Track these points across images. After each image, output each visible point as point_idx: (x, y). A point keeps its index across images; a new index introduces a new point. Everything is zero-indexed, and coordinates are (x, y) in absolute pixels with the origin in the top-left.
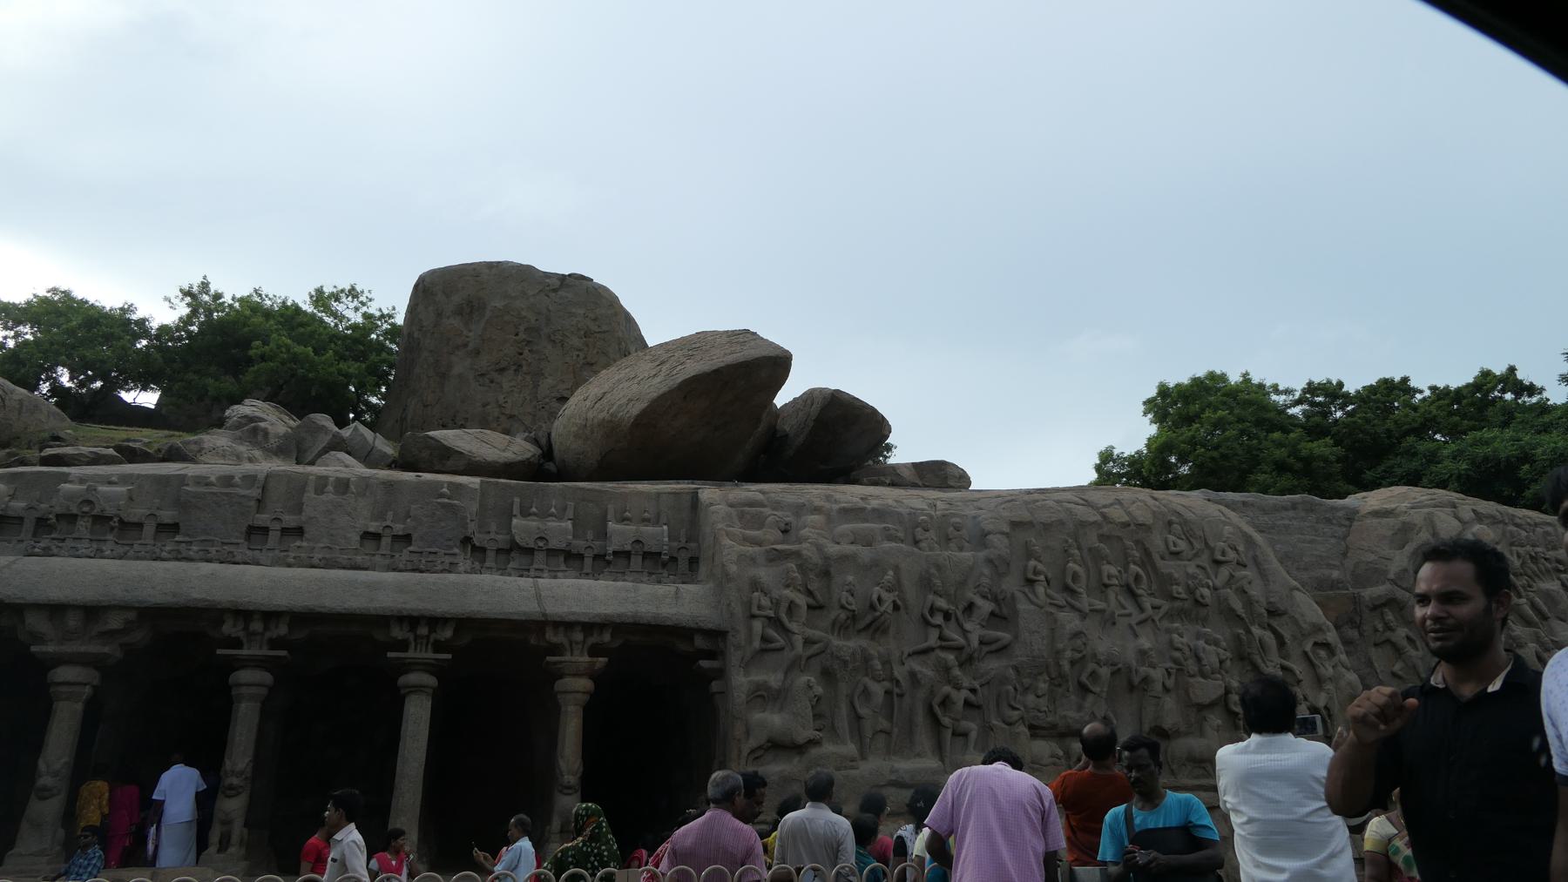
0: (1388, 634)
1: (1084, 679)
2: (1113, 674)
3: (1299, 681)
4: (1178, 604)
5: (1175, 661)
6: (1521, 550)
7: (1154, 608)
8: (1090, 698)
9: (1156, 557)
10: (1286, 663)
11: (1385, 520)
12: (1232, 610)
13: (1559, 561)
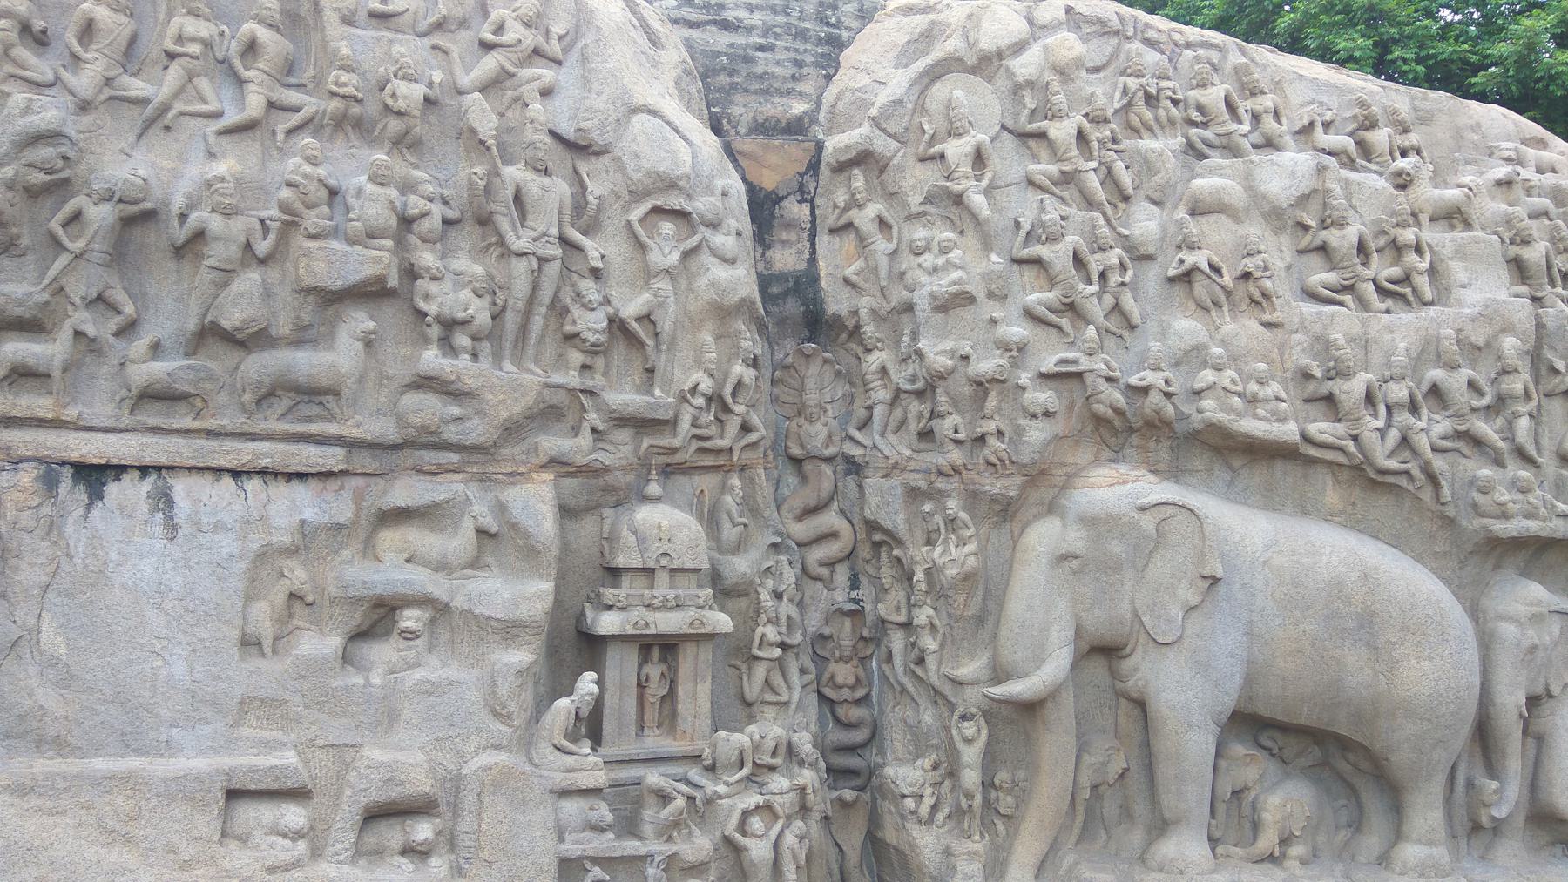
0: (853, 213)
1: (55, 225)
2: (128, 222)
3: (596, 274)
4: (335, 105)
5: (284, 207)
6: (1132, 83)
7: (271, 105)
8: (64, 259)
9: (331, 19)
10: (575, 235)
11: (906, 20)
12: (473, 131)
13: (1200, 108)
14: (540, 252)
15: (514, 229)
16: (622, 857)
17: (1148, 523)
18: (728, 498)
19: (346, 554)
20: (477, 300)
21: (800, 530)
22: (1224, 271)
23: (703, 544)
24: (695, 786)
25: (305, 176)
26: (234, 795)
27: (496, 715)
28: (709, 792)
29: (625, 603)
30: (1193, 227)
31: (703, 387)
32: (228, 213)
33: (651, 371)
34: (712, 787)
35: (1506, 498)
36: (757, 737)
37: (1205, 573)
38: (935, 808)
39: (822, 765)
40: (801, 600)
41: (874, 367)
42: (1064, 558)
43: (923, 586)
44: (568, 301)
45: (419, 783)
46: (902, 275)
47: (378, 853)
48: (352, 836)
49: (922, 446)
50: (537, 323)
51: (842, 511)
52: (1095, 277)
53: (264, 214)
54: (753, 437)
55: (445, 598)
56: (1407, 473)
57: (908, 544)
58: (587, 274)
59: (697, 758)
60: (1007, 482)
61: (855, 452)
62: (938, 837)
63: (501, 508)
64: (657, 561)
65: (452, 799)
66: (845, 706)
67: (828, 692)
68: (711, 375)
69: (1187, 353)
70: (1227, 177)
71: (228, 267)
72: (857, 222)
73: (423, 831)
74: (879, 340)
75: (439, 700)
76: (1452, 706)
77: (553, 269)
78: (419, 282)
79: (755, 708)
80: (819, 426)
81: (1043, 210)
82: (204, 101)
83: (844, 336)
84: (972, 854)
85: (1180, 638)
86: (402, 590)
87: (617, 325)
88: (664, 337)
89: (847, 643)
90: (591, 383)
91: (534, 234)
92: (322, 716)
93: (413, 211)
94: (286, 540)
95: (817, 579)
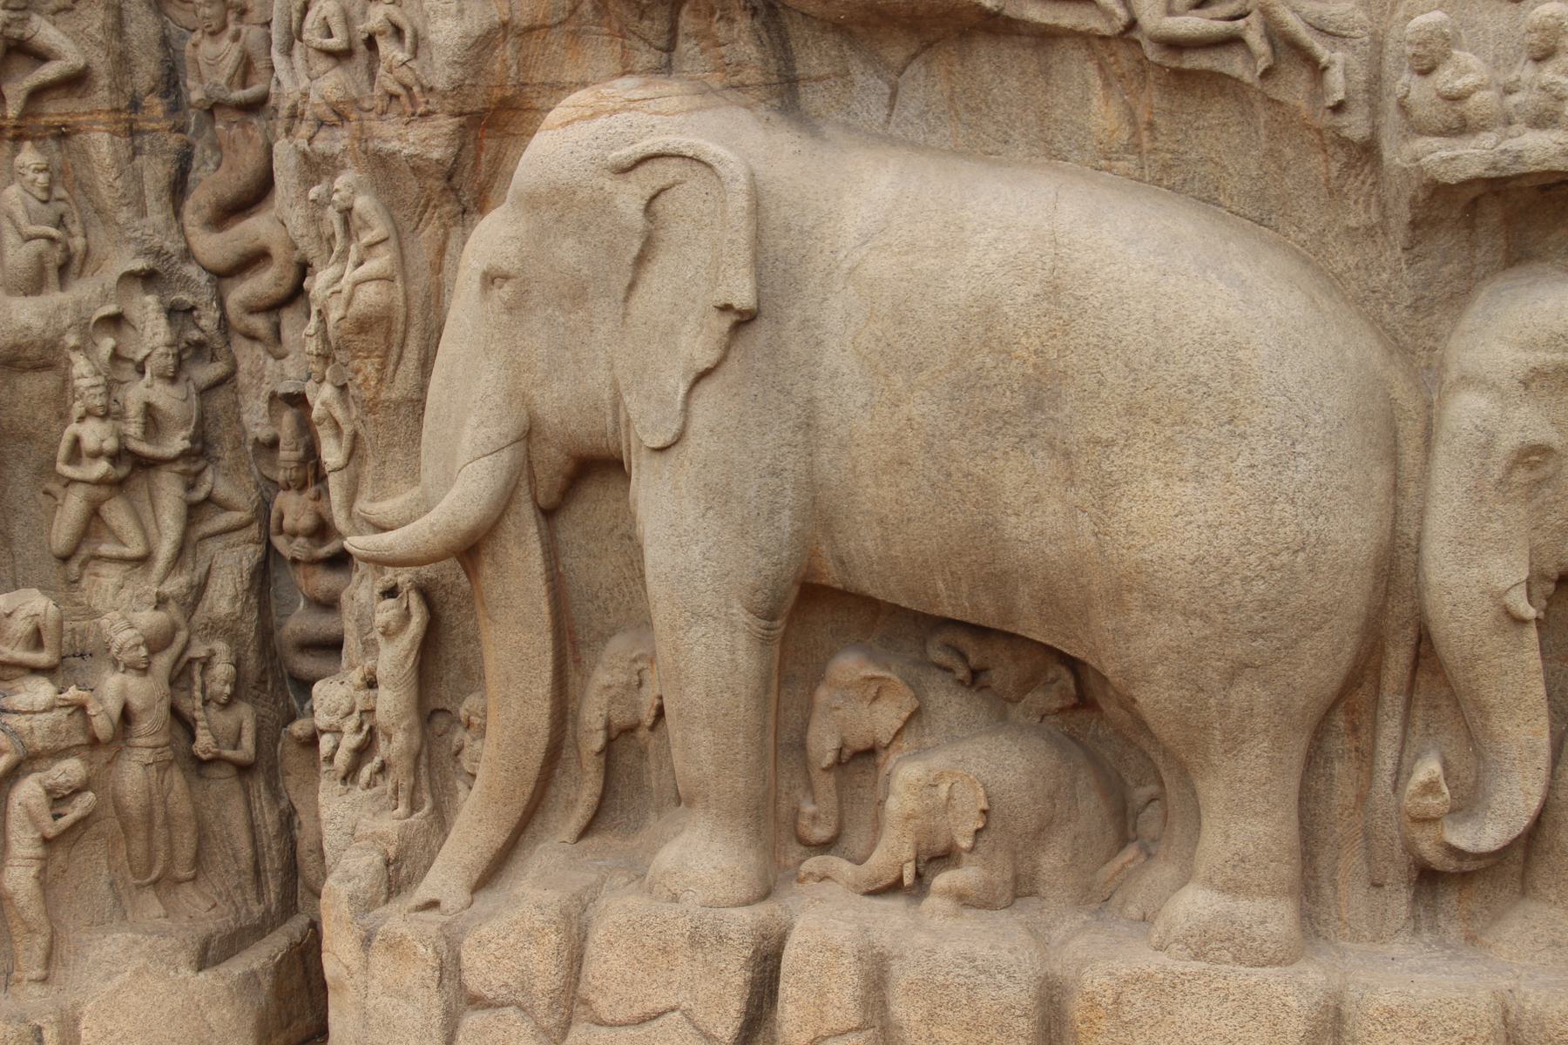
17: (629, 197)
21: (215, 247)
35: (1470, 80)
37: (721, 297)
38: (362, 752)
39: (222, 669)
40: (227, 380)
42: (491, 279)
43: (313, 345)
54: (49, 72)
56: (1232, 41)
57: (316, 263)
62: (353, 806)
66: (300, 570)
67: (280, 542)
76: (1259, 587)
79: (74, 567)
80: (225, 42)
85: (679, 438)
89: (287, 454)
95: (252, 337)
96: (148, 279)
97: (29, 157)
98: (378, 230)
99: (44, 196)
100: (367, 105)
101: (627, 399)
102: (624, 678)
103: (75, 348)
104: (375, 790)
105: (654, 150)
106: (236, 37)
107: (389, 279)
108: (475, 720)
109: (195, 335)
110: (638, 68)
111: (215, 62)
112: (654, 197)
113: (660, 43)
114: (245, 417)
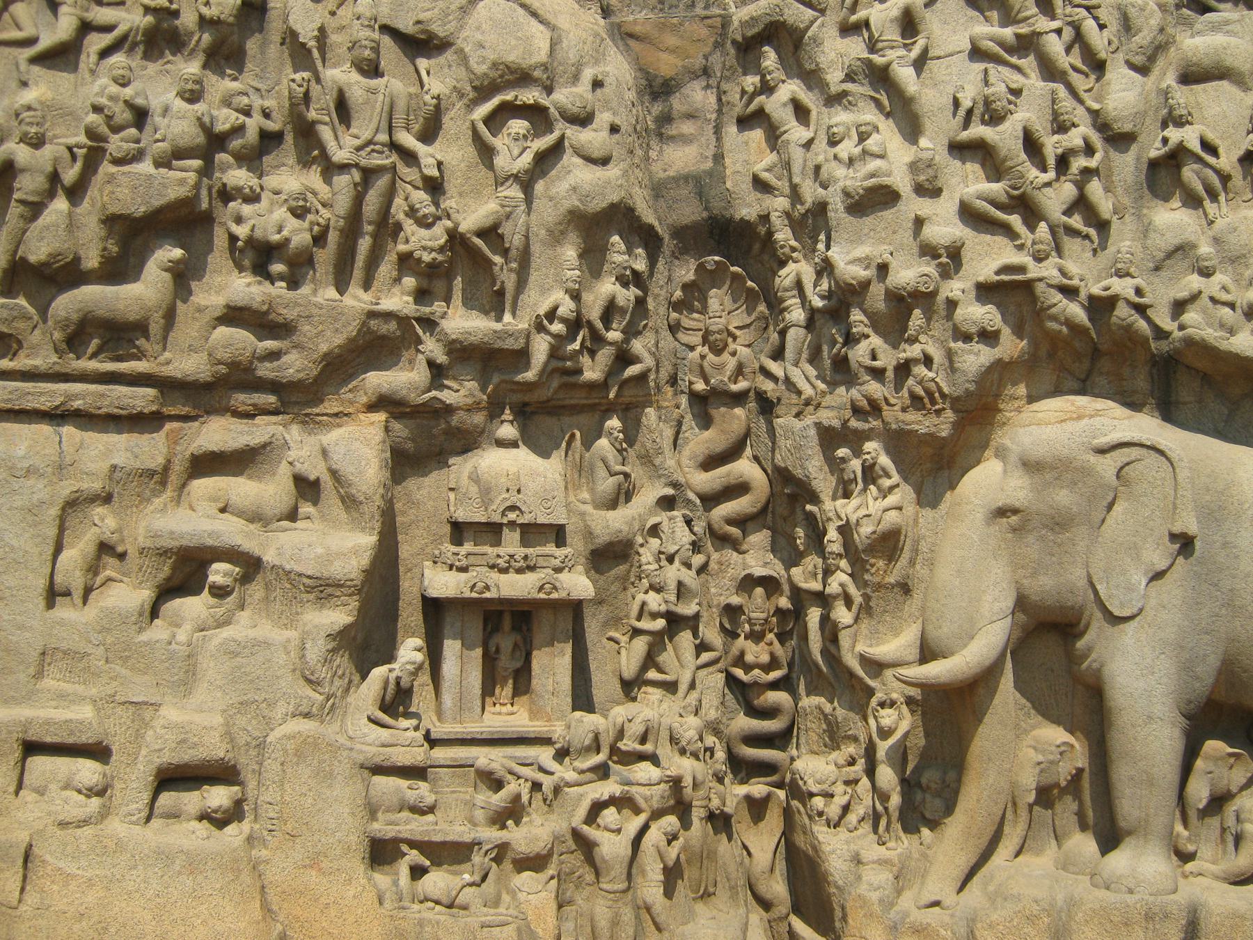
10: (408, 140)
14: (363, 162)
15: (337, 138)
16: (444, 843)
17: (1107, 466)
18: (603, 442)
19: (158, 502)
20: (292, 223)
22: (1221, 151)
23: (560, 494)
24: (542, 769)
25: (111, 98)
26: (32, 748)
27: (309, 681)
28: (555, 777)
29: (464, 563)
30: (1183, 97)
31: (561, 311)
32: (37, 142)
33: (501, 293)
34: (565, 772)
36: (620, 720)
37: (1177, 529)
38: (846, 809)
39: (720, 755)
41: (787, 282)
42: (1002, 512)
43: (836, 547)
44: (401, 216)
45: (213, 748)
46: (818, 168)
47: (174, 815)
48: (146, 796)
49: (838, 377)
50: (364, 244)
51: (756, 459)
52: (1051, 161)
53: (72, 141)
55: (257, 552)
57: (823, 496)
58: (420, 184)
59: (546, 741)
60: (936, 420)
61: (768, 386)
62: (847, 842)
63: (325, 453)
64: (503, 514)
65: (256, 767)
68: (576, 296)
69: (1170, 255)
70: (1235, 34)
71: (31, 199)
72: (768, 109)
73: (218, 796)
74: (794, 249)
75: (244, 660)
77: (382, 182)
78: (232, 204)
81: (986, 83)
82: (19, 28)
83: (757, 246)
84: (883, 862)
85: (1141, 610)
86: (210, 542)
87: (455, 238)
88: (513, 253)
90: (427, 310)
91: (357, 142)
92: (124, 671)
93: (221, 127)
94: (96, 486)
96: (667, 503)
97: (614, 423)
98: (896, 478)
99: (618, 447)
100: (892, 401)
101: (1098, 587)
102: (1051, 757)
103: (642, 545)
104: (860, 831)
105: (1126, 440)
106: (734, 354)
107: (900, 509)
108: (933, 786)
109: (694, 538)
110: (1065, 389)
111: (720, 368)
112: (1122, 468)
113: (1083, 376)
114: (713, 590)
